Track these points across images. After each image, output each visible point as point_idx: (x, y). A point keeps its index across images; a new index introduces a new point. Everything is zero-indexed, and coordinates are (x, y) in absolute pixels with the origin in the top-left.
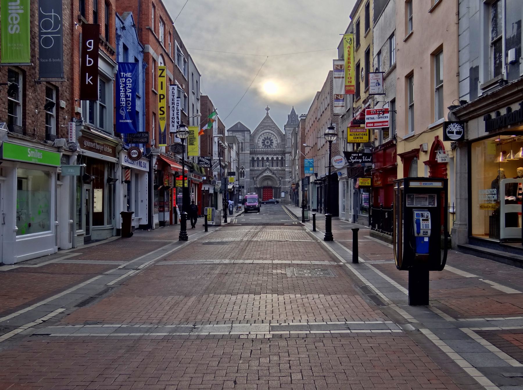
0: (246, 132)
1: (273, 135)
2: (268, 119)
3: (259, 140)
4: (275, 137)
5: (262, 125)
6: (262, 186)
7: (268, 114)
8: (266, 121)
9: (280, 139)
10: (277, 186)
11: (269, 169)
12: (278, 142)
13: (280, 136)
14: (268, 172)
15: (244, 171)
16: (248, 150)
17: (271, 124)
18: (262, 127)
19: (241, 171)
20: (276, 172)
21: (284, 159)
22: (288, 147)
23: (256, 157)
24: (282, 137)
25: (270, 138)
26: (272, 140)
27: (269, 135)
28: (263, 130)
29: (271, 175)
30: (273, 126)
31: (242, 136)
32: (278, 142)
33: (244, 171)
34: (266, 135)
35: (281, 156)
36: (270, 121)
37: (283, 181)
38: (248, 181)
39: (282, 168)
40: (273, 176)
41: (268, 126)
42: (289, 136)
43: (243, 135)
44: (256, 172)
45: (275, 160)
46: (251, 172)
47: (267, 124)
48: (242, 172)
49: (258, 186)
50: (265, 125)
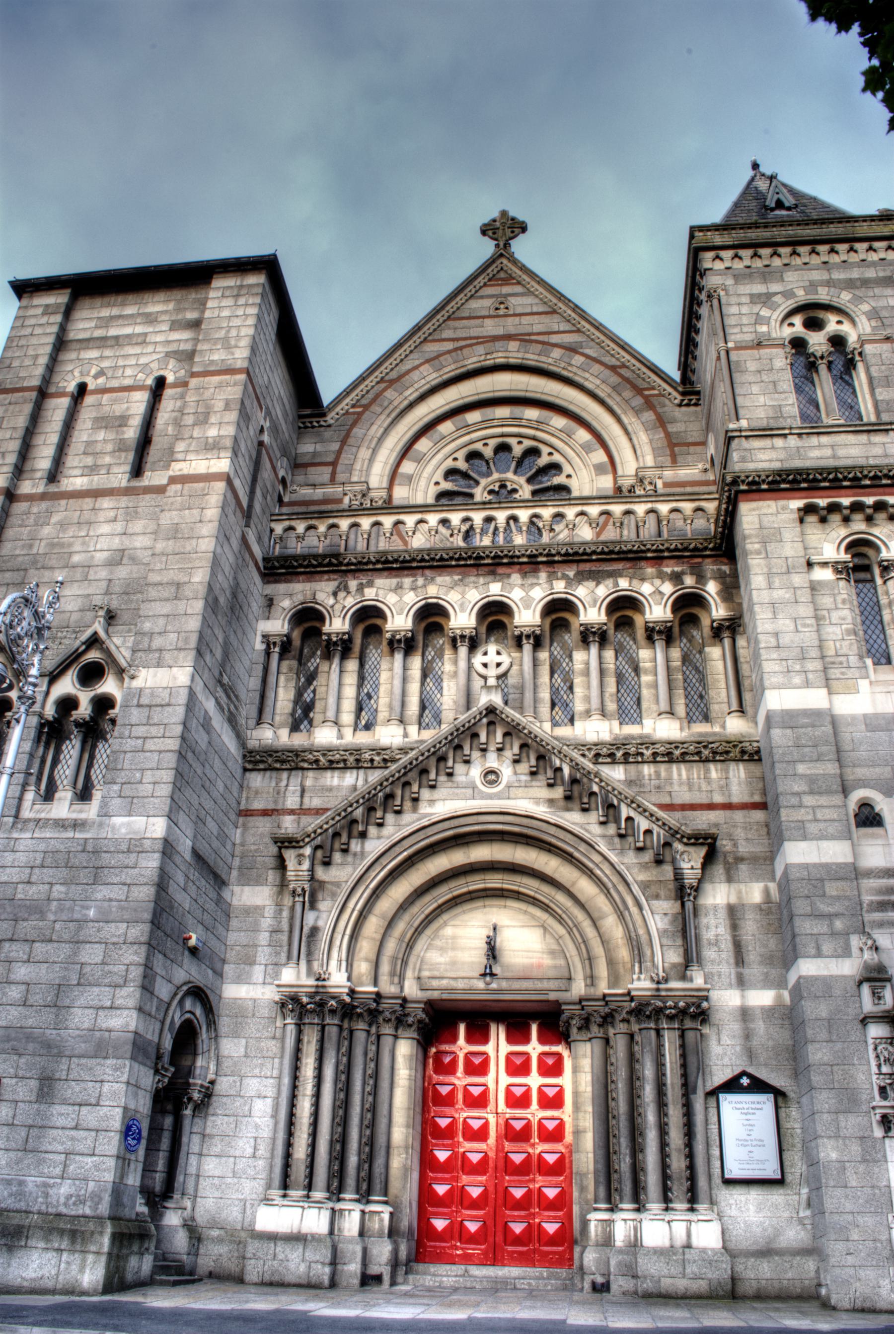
0: (220, 283)
1: (559, 422)
2: (506, 290)
3: (408, 467)
4: (583, 435)
5: (447, 334)
6: (411, 989)
7: (503, 252)
8: (487, 303)
9: (642, 438)
10: (641, 985)
11: (512, 730)
12: (628, 466)
13: (637, 412)
14: (491, 776)
15: (103, 704)
16: (211, 447)
17: (538, 324)
18: (450, 346)
19: (68, 704)
20: (616, 774)
21: (719, 611)
22: (766, 432)
23: (350, 602)
24: (662, 422)
25: (533, 452)
26: (555, 467)
27: (516, 421)
28: (450, 370)
29: (541, 811)
30: (554, 339)
31: (175, 326)
32: (628, 466)
33: (103, 704)
34: (486, 424)
35: (676, 578)
36: (529, 300)
37: (733, 912)
38: (135, 846)
39: (700, 728)
40: (573, 819)
41: (509, 337)
42: (759, 320)
43: (191, 315)
44: (332, 779)
45: (587, 636)
46: (257, 780)
47: (491, 327)
48: (84, 710)
49: (338, 980)
50: (474, 332)
